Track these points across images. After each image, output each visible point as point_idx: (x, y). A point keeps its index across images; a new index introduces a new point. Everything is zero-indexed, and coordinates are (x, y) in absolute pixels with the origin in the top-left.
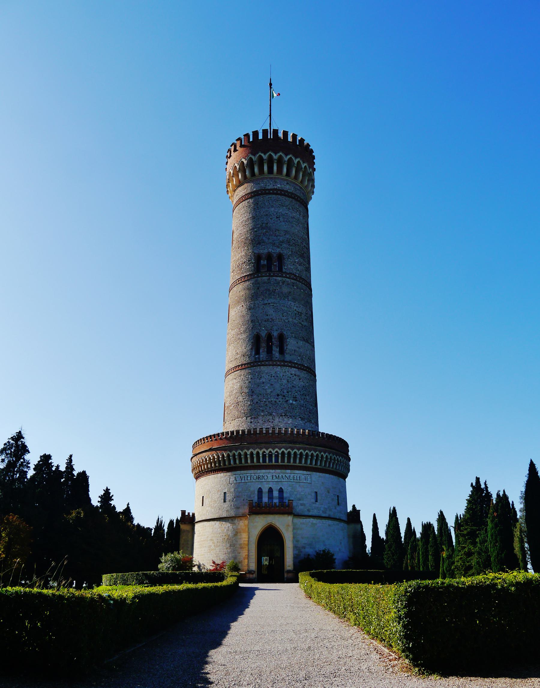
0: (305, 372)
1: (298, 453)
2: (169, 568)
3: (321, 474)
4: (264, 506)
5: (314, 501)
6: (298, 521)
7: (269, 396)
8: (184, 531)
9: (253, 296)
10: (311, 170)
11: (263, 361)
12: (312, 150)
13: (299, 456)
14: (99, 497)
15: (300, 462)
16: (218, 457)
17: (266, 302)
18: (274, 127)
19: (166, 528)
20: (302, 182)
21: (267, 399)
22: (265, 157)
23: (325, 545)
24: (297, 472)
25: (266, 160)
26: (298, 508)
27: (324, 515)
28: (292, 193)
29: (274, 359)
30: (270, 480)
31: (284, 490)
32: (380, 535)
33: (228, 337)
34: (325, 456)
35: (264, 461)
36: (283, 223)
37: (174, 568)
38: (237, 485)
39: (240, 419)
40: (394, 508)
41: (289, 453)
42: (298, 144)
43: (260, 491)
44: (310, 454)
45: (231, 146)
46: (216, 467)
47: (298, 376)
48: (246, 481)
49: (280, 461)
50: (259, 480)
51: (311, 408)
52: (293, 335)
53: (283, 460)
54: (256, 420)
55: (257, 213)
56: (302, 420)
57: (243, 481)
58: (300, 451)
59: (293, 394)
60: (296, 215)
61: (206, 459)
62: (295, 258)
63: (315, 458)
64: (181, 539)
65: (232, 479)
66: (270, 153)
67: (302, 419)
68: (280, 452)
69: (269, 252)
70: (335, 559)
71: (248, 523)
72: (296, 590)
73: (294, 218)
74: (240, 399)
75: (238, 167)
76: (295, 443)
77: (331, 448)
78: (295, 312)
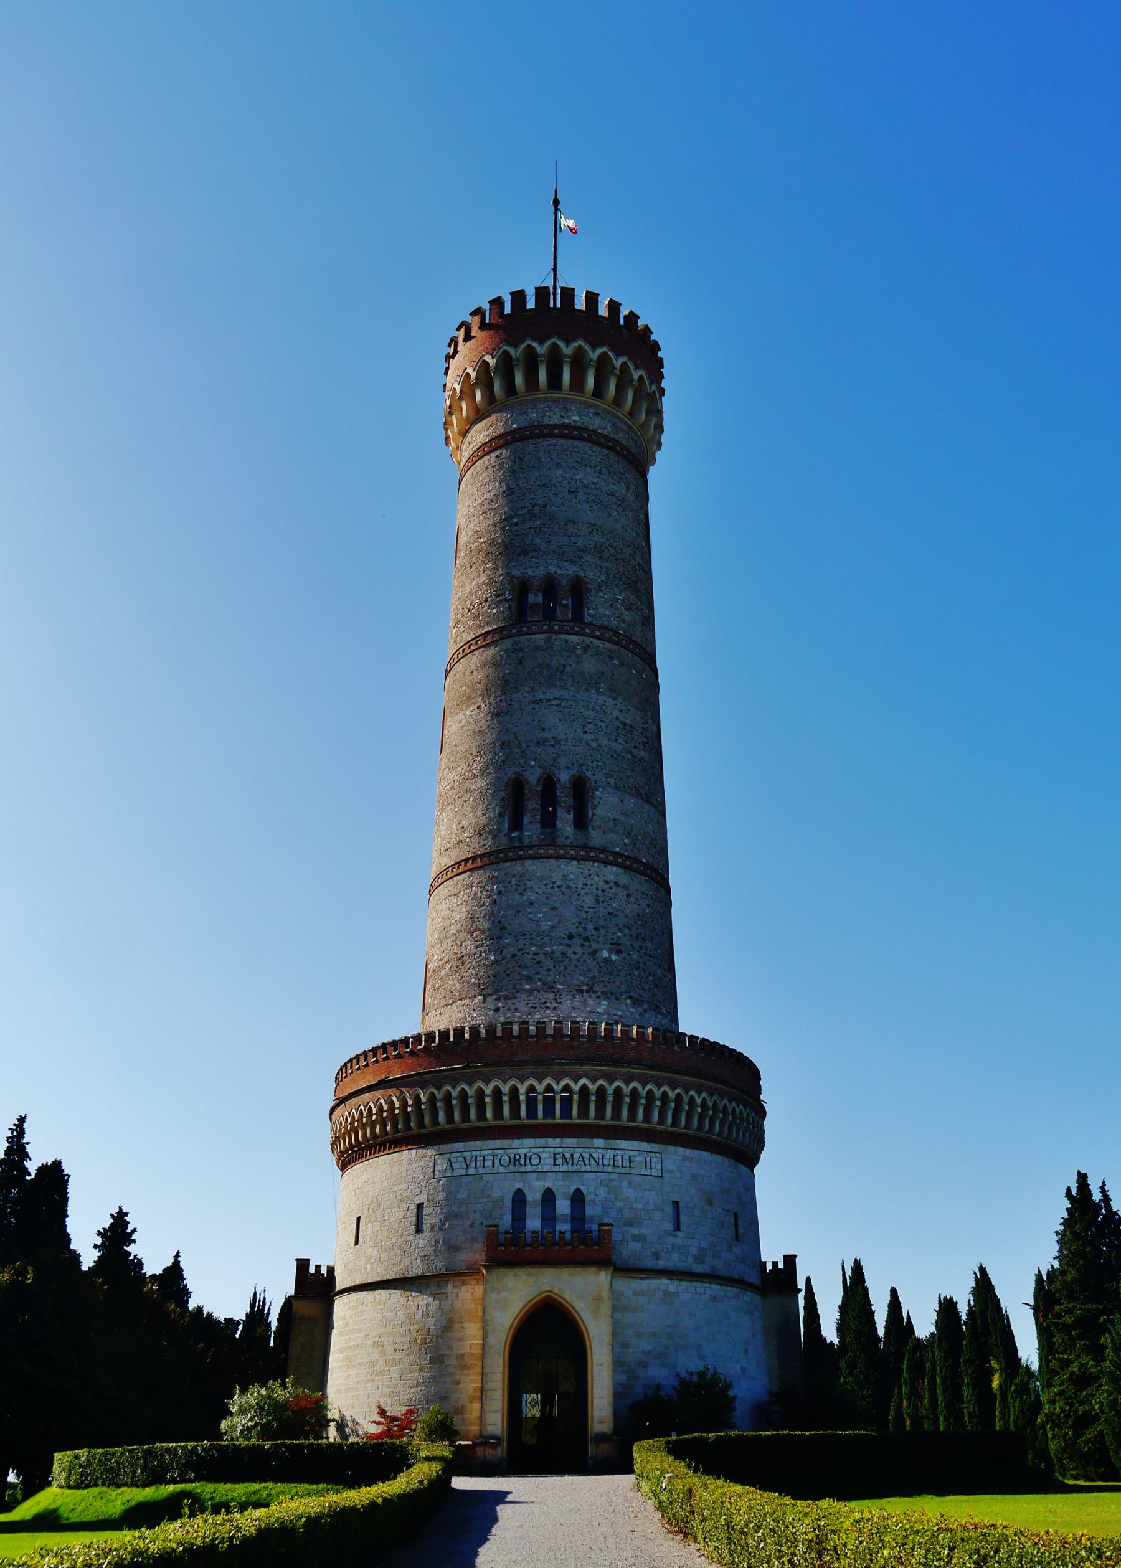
0: (643, 878)
1: (627, 1090)
3: (688, 1151)
4: (529, 1240)
5: (669, 1227)
6: (628, 1286)
7: (546, 939)
9: (506, 682)
10: (654, 388)
11: (530, 847)
12: (656, 343)
13: (627, 1099)
14: (99, 1233)
15: (632, 1116)
17: (542, 696)
18: (561, 283)
19: (274, 1320)
20: (632, 413)
21: (541, 947)
22: (541, 349)
23: (702, 1357)
24: (623, 1144)
25: (543, 356)
26: (628, 1250)
27: (697, 1268)
28: (607, 438)
29: (560, 841)
31: (588, 1197)
33: (439, 789)
34: (699, 1101)
36: (586, 506)
38: (453, 1183)
39: (467, 1001)
41: (601, 1091)
42: (622, 323)
43: (519, 1199)
44: (658, 1093)
45: (458, 329)
46: (397, 1131)
47: (625, 887)
48: (481, 1171)
49: (575, 1112)
50: (516, 1169)
51: (659, 972)
52: (612, 781)
53: (584, 1112)
54: (510, 1002)
55: (520, 483)
56: (634, 1003)
57: (471, 1171)
58: (631, 1086)
59: (610, 935)
60: (619, 489)
62: (616, 590)
63: (673, 1105)
66: (554, 340)
67: (636, 1002)
68: (576, 1087)
69: (549, 574)
71: (485, 1291)
73: (612, 494)
74: (469, 947)
75: (473, 375)
76: (616, 1063)
77: (715, 1079)
78: (617, 723)
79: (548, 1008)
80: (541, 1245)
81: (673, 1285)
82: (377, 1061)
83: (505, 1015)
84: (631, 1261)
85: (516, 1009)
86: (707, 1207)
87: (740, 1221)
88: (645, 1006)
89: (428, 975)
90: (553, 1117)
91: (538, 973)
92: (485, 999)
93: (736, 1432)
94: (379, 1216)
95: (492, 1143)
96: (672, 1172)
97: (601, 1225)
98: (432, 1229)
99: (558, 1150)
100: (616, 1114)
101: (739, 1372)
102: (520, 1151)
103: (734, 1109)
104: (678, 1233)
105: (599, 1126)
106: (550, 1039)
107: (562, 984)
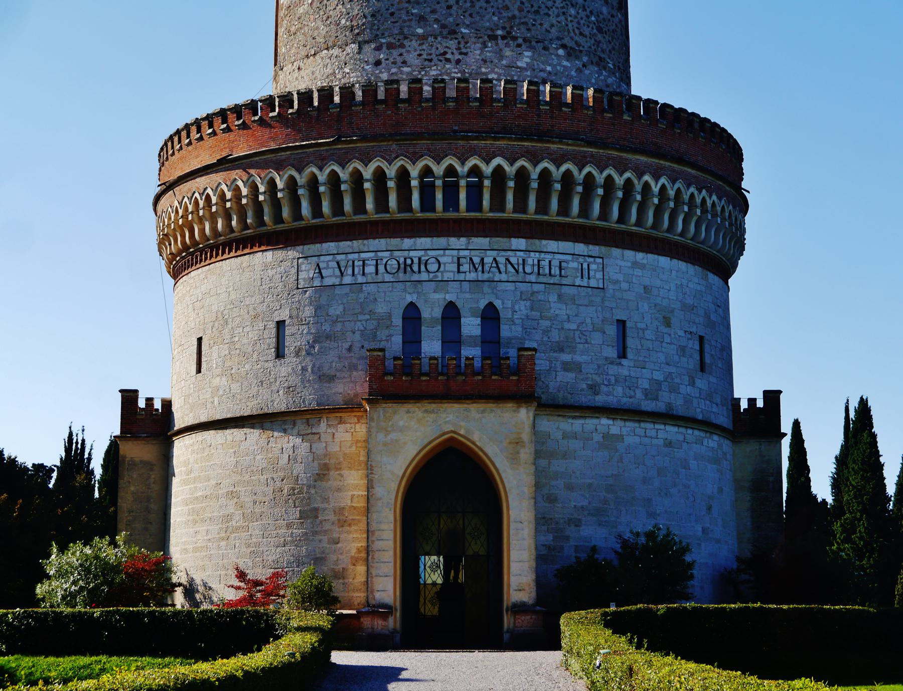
2: (73, 595)
3: (640, 256)
5: (612, 353)
6: (556, 426)
8: (133, 464)
13: (558, 186)
15: (564, 209)
16: (254, 188)
23: (651, 515)
24: (552, 245)
26: (557, 381)
27: (649, 406)
30: (447, 271)
32: (814, 489)
34: (656, 189)
35: (427, 203)
37: (94, 598)
38: (323, 295)
39: (336, 51)
40: (863, 403)
41: (522, 175)
43: (412, 317)
44: (600, 178)
46: (246, 227)
48: (360, 279)
49: (486, 203)
50: (407, 277)
51: (605, 10)
54: (395, 53)
57: (348, 279)
58: (563, 168)
61: (208, 196)
63: (620, 194)
64: (121, 494)
65: (307, 271)
67: (571, 53)
68: (487, 169)
70: (691, 565)
71: (369, 432)
72: (550, 678)
76: (543, 136)
77: (680, 160)
79: (448, 60)
80: (442, 374)
81: (615, 427)
82: (214, 133)
83: (389, 70)
84: (561, 395)
85: (404, 62)
86: (663, 329)
87: (707, 347)
88: (585, 59)
89: (281, 14)
90: (457, 209)
91: (434, 11)
92: (360, 48)
93: (693, 604)
94: (227, 337)
95: (374, 244)
96: (616, 282)
97: (520, 349)
98: (297, 354)
99: (462, 253)
100: (543, 206)
101: (700, 533)
102: (412, 254)
103: (704, 200)
104: (624, 362)
105: (519, 221)
106: (451, 104)
107: (467, 27)
